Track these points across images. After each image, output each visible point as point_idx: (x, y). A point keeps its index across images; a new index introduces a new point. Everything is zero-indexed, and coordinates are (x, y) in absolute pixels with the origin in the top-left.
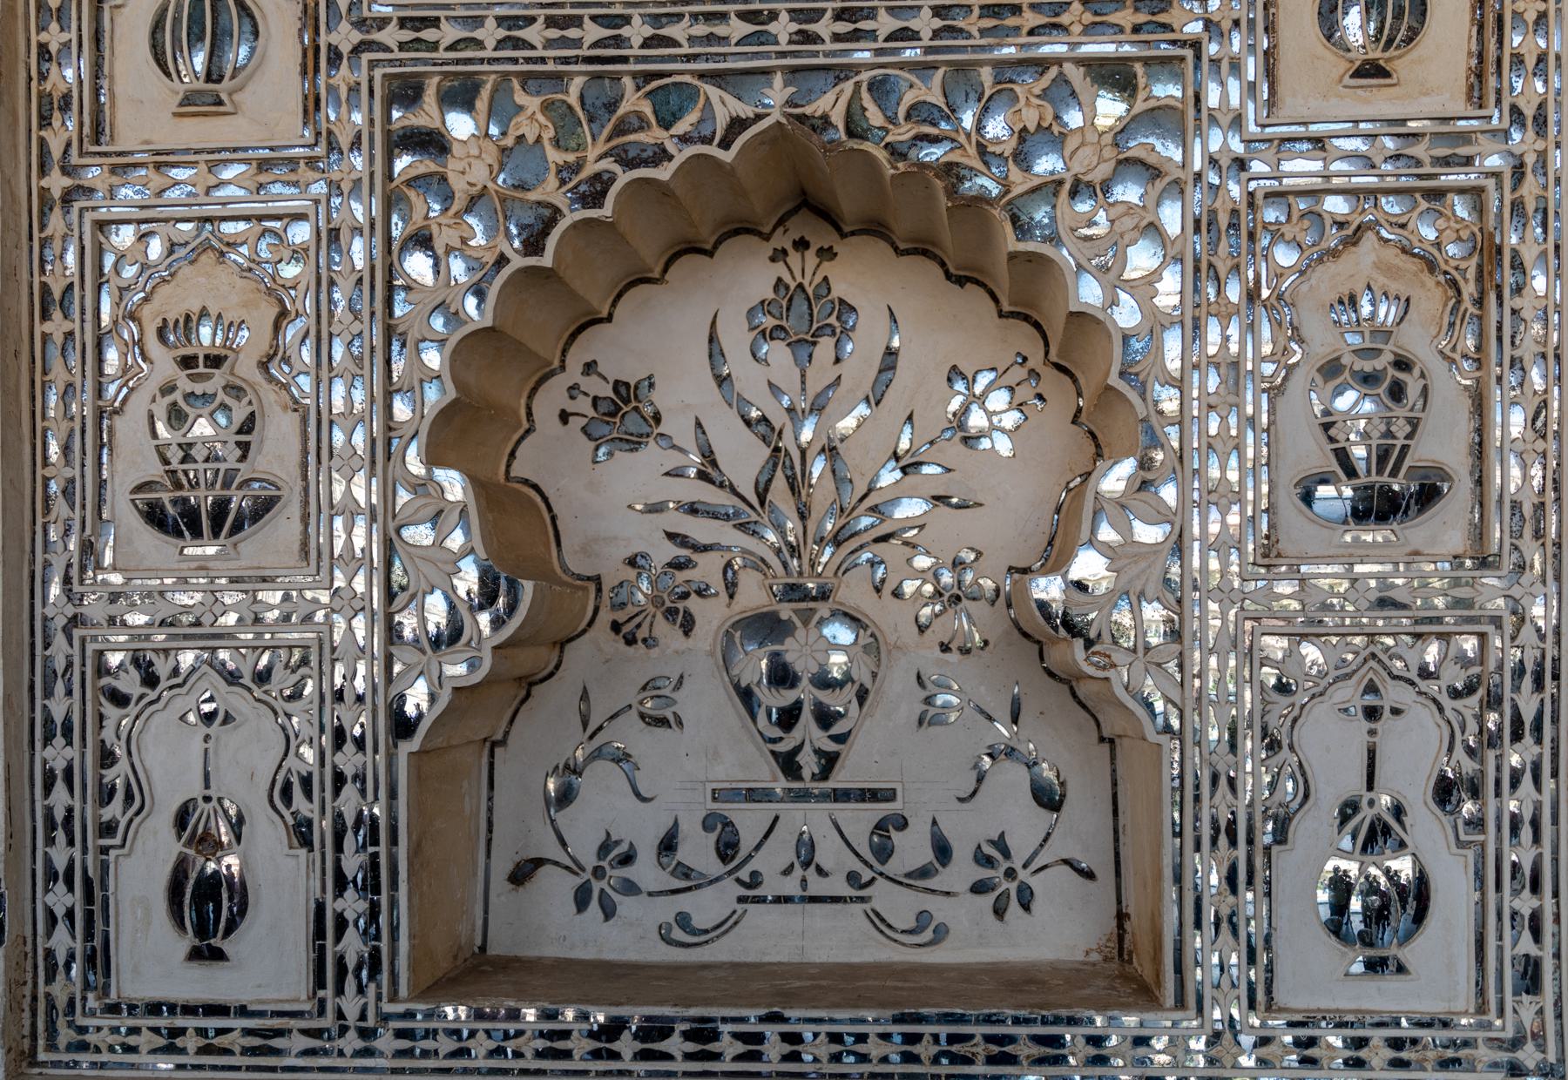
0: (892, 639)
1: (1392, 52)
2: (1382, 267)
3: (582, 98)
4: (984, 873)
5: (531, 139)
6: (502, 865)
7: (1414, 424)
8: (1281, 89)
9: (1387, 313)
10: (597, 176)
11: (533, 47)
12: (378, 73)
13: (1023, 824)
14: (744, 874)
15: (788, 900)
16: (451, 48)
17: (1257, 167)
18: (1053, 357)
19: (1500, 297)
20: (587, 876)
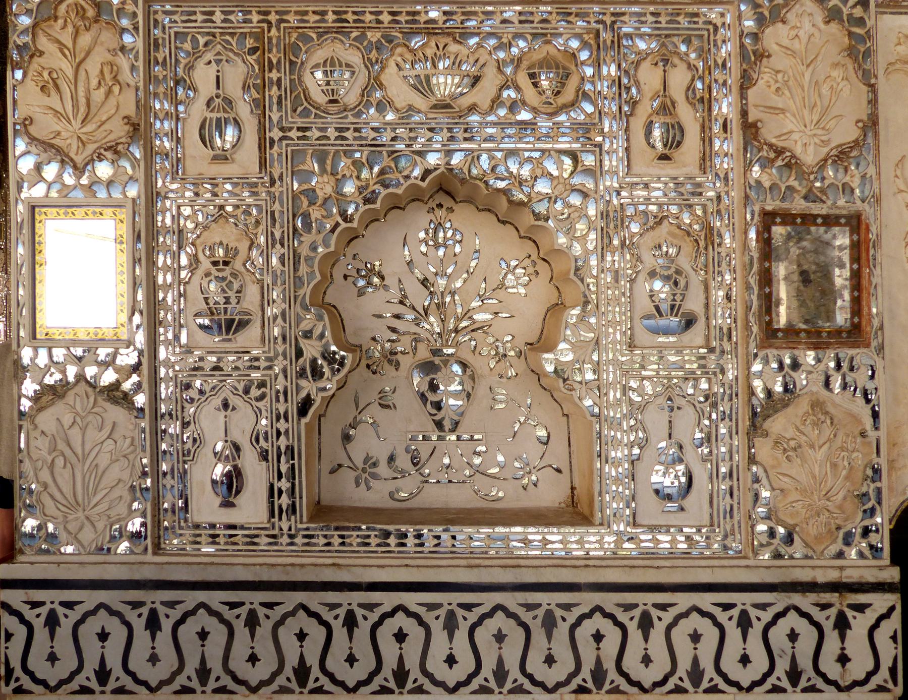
0: (479, 372)
3: (367, 160)
5: (348, 175)
7: (684, 296)
9: (672, 251)
10: (374, 191)
12: (289, 149)
16: (317, 139)
19: (713, 247)
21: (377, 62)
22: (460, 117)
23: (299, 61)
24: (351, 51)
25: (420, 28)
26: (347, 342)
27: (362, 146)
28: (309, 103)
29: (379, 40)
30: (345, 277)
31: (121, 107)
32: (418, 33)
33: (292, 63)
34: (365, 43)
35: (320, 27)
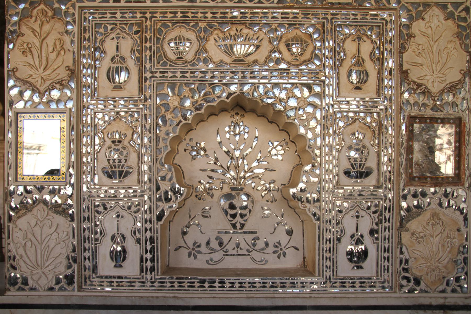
0: (256, 199)
1: (362, 85)
2: (359, 127)
3: (197, 88)
4: (276, 249)
5: (187, 96)
6: (172, 248)
8: (340, 91)
9: (361, 137)
10: (201, 104)
11: (188, 78)
12: (155, 83)
13: (284, 239)
14: (224, 250)
15: (234, 255)
16: (170, 77)
17: (335, 106)
18: (291, 139)
20: (191, 250)
21: (204, 38)
22: (248, 66)
23: (162, 38)
24: (190, 32)
25: (228, 21)
26: (186, 184)
27: (194, 81)
28: (167, 59)
29: (205, 27)
31: (64, 62)
32: (227, 23)
33: (158, 39)
34: (198, 28)
35: (173, 20)
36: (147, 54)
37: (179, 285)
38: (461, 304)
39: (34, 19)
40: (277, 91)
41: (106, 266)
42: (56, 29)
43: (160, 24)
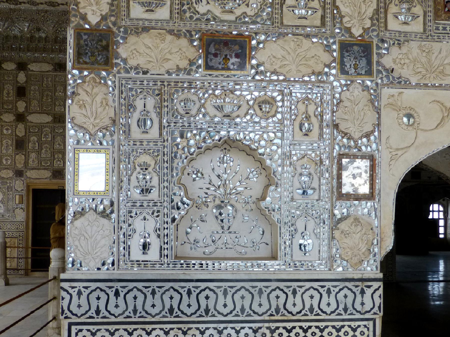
30: (188, 174)
36: (165, 110)
37: (186, 266)
38: (373, 277)
39: (87, 84)
40: (252, 135)
41: (136, 254)
42: (102, 92)
43: (174, 90)
